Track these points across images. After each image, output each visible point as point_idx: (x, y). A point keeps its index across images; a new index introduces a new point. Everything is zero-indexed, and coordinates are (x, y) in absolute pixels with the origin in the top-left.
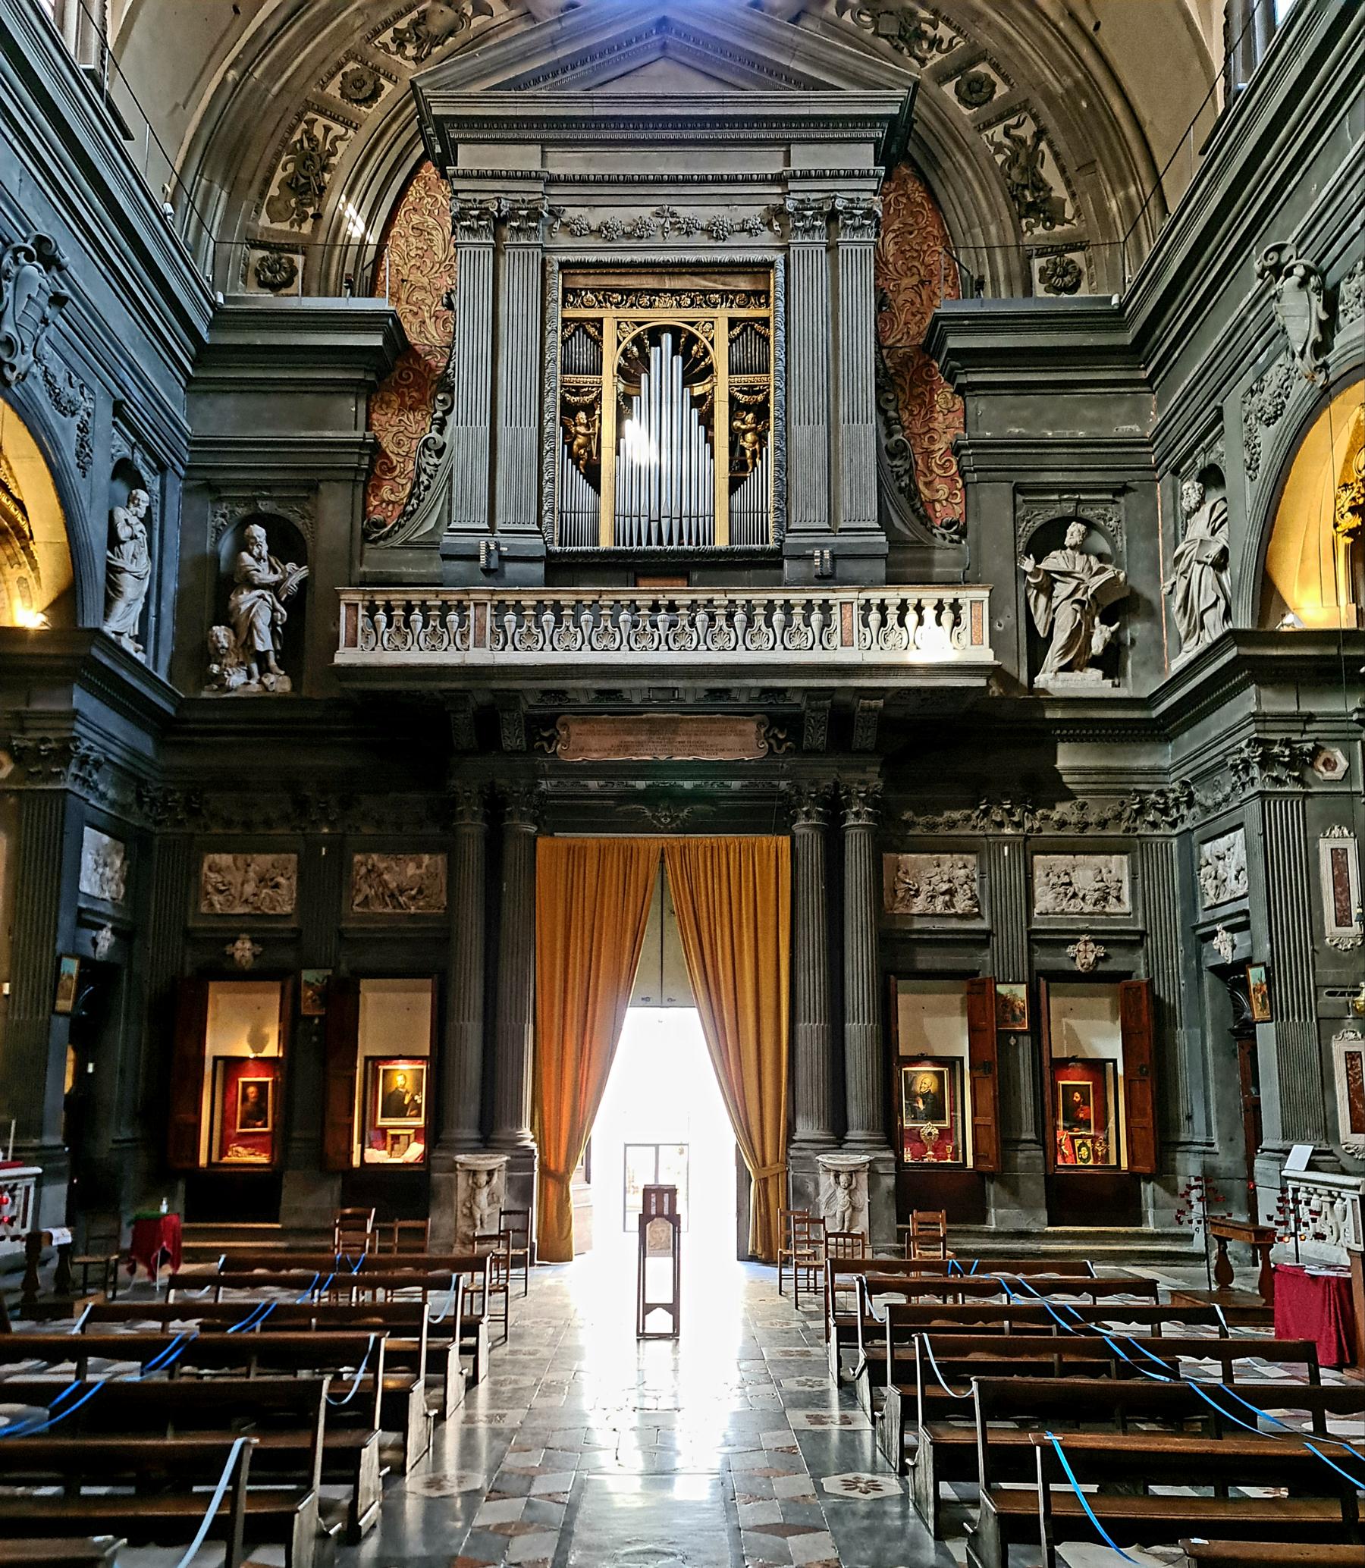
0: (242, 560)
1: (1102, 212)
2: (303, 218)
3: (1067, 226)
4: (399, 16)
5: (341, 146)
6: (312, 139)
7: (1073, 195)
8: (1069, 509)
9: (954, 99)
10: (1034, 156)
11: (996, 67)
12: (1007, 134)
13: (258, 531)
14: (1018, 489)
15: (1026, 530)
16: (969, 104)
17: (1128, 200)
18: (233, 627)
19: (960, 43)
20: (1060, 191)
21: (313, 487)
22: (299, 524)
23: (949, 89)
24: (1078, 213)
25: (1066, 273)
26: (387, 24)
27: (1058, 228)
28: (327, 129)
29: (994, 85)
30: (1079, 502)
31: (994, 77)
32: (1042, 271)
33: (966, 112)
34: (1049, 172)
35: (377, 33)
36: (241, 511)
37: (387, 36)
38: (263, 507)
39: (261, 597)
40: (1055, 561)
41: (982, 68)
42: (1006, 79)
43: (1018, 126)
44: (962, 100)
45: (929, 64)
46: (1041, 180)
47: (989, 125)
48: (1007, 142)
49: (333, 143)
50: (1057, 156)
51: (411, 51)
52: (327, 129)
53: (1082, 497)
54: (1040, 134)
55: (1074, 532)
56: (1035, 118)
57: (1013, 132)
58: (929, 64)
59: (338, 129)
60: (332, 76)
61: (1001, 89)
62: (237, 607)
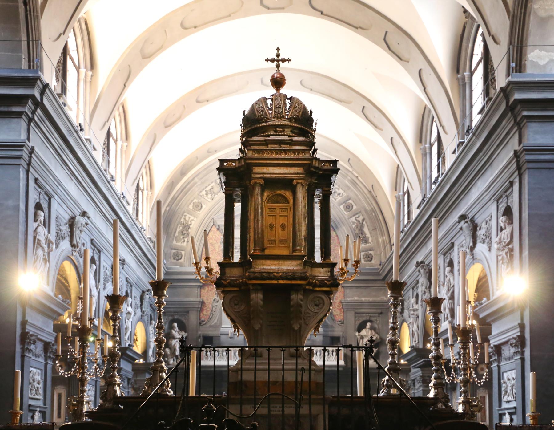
0: (172, 332)
1: (378, 242)
2: (184, 241)
3: (370, 244)
4: (206, 187)
5: (193, 222)
6: (185, 220)
7: (371, 236)
8: (368, 318)
9: (343, 209)
10: (362, 226)
11: (354, 201)
12: (356, 220)
13: (176, 325)
14: (356, 313)
15: (358, 323)
16: (347, 211)
17: (383, 241)
18: (170, 348)
19: (345, 194)
20: (368, 235)
21: (188, 312)
22: (184, 321)
23: (342, 207)
24: (372, 241)
25: (369, 257)
26: (203, 189)
27: (367, 245)
28: (189, 218)
29: (352, 206)
30: (370, 316)
31: (353, 204)
32: (363, 256)
33: (346, 213)
34: (366, 230)
35: (201, 192)
36: (171, 318)
37: (204, 193)
38: (176, 317)
39: (177, 341)
40: (364, 332)
41: (350, 201)
42: (356, 205)
43: (358, 217)
44: (345, 210)
45: (337, 200)
46: (363, 232)
47: (351, 217)
48: (356, 221)
49: (191, 221)
50: (367, 226)
51: (209, 196)
52: (189, 218)
53: (372, 315)
54: (363, 220)
55: (369, 324)
56: (363, 215)
57: (358, 219)
58: (337, 200)
59: (192, 218)
60: (190, 204)
61: (355, 207)
62: (171, 344)
